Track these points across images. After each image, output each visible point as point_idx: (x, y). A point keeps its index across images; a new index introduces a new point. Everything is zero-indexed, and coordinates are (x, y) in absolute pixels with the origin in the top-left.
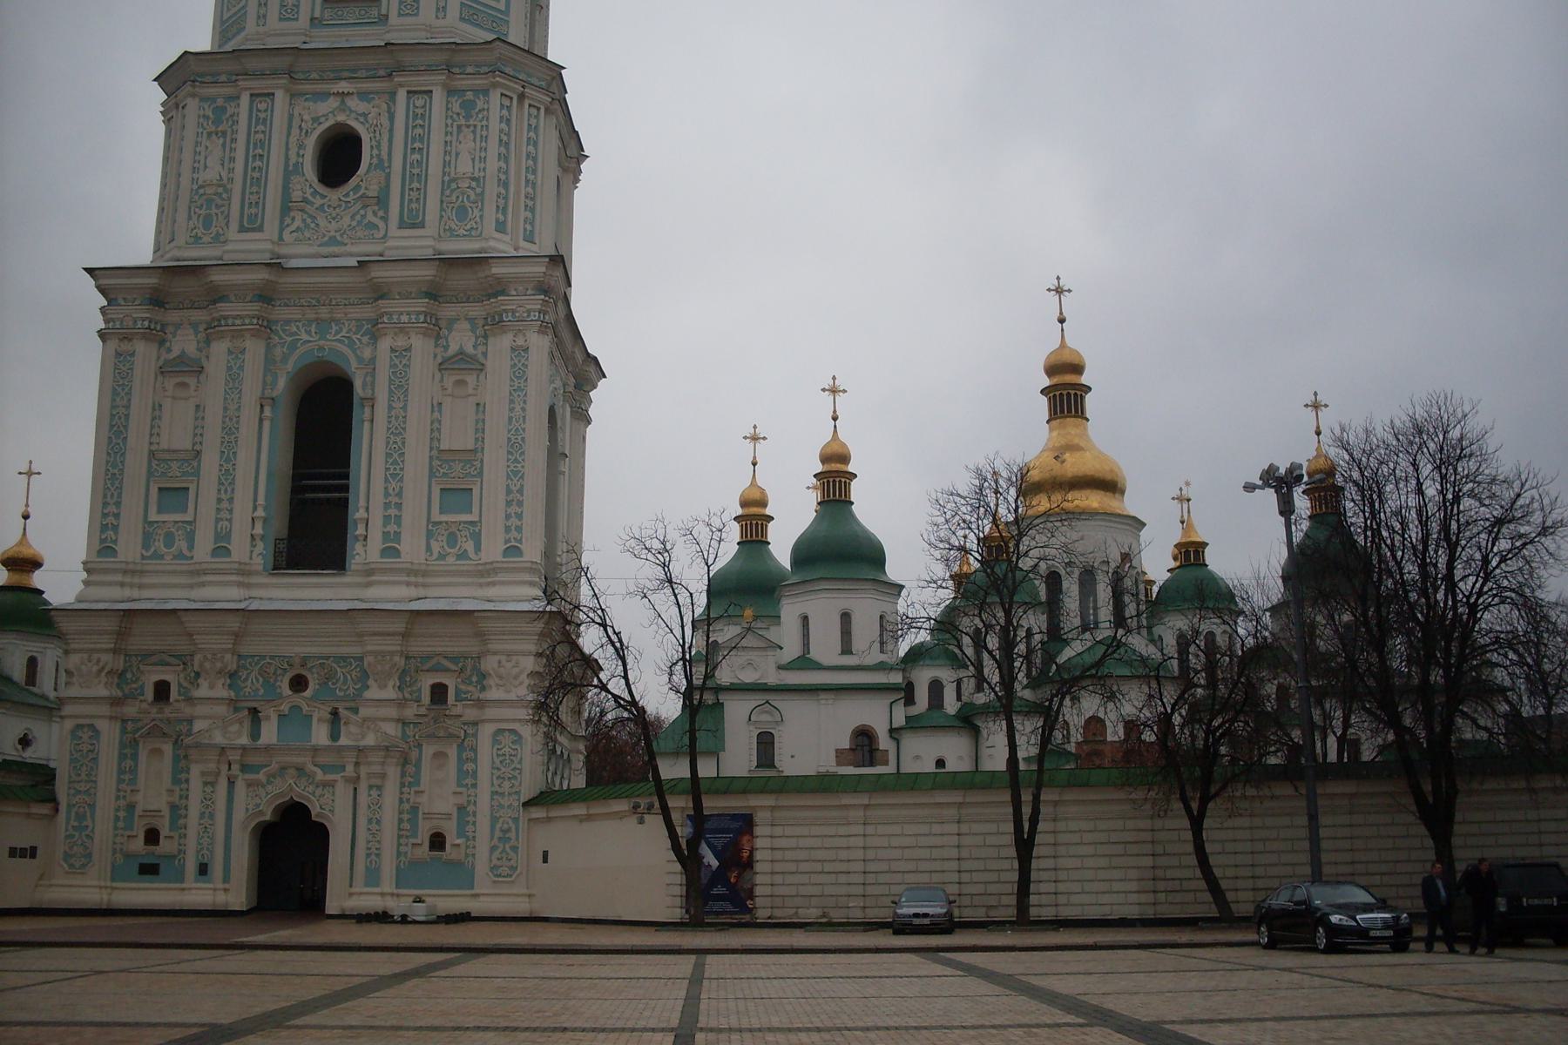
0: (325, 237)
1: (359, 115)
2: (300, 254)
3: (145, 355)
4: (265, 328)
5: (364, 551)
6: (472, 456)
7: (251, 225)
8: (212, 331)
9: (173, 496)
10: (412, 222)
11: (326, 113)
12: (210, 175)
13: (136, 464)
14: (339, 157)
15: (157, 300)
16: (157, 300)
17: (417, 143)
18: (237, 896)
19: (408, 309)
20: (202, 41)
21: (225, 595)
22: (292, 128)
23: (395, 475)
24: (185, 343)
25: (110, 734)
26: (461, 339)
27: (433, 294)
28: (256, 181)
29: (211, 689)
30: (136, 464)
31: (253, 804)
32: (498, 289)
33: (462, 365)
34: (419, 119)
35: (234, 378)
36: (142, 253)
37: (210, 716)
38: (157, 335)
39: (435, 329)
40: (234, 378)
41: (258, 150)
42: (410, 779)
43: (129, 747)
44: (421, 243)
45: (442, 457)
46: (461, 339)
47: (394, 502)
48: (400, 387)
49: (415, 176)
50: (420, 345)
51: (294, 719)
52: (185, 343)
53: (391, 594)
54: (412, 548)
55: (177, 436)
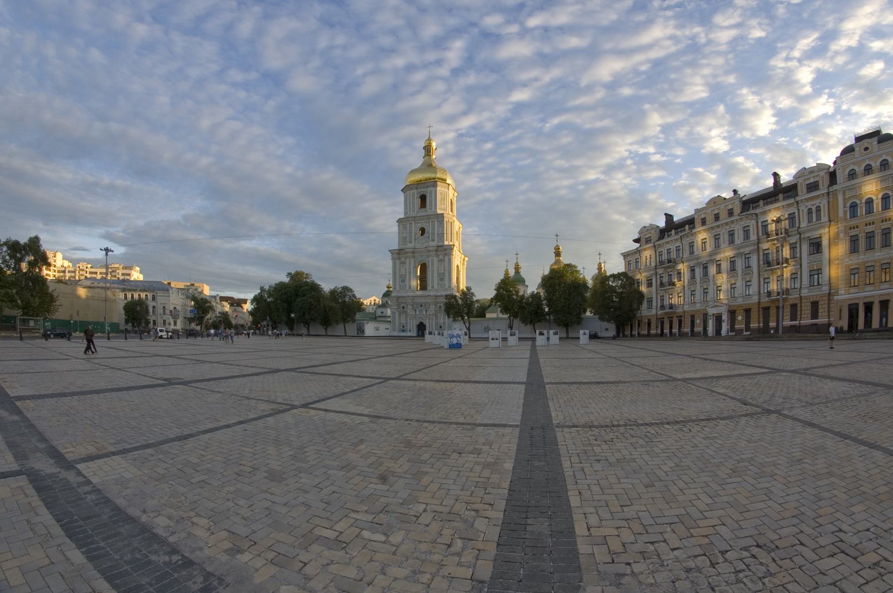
1: (424, 225)
2: (418, 246)
3: (398, 262)
5: (429, 288)
7: (411, 242)
9: (403, 281)
10: (433, 240)
13: (398, 277)
14: (423, 231)
15: (399, 254)
16: (399, 254)
17: (433, 229)
18: (415, 334)
20: (403, 216)
22: (415, 228)
23: (433, 277)
24: (403, 259)
25: (397, 314)
26: (441, 257)
27: (436, 251)
30: (398, 277)
31: (415, 323)
32: (446, 250)
35: (410, 264)
36: (397, 247)
37: (409, 310)
38: (399, 259)
39: (437, 256)
40: (410, 264)
41: (411, 232)
42: (436, 319)
43: (400, 315)
44: (432, 244)
45: (439, 274)
46: (441, 257)
47: (433, 280)
48: (433, 264)
49: (433, 234)
50: (435, 259)
51: (421, 311)
52: (403, 259)
53: (432, 293)
54: (436, 287)
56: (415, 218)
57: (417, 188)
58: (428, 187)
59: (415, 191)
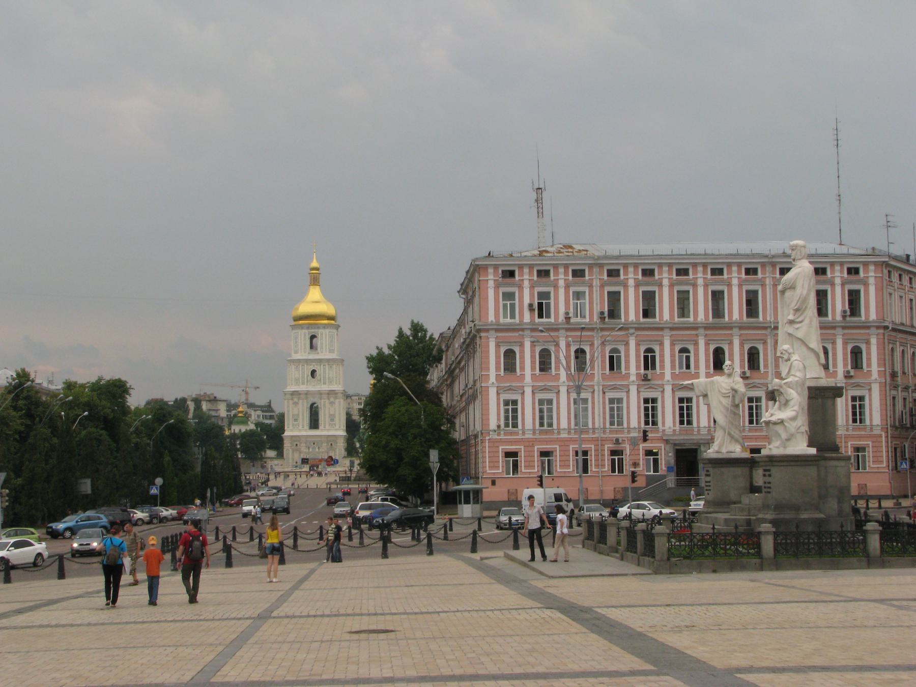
0: (313, 387)
2: (311, 388)
4: (307, 398)
5: (321, 427)
6: (334, 415)
8: (299, 399)
11: (311, 368)
12: (297, 376)
14: (313, 373)
19: (325, 396)
21: (304, 433)
24: (296, 400)
26: (332, 400)
28: (303, 377)
29: (303, 445)
33: (332, 403)
34: (324, 369)
41: (303, 373)
45: (330, 415)
46: (332, 400)
49: (324, 377)
50: (327, 401)
51: (314, 448)
52: (296, 400)
55: (296, 412)
56: (308, 361)
57: (308, 328)
58: (319, 328)
59: (307, 331)
